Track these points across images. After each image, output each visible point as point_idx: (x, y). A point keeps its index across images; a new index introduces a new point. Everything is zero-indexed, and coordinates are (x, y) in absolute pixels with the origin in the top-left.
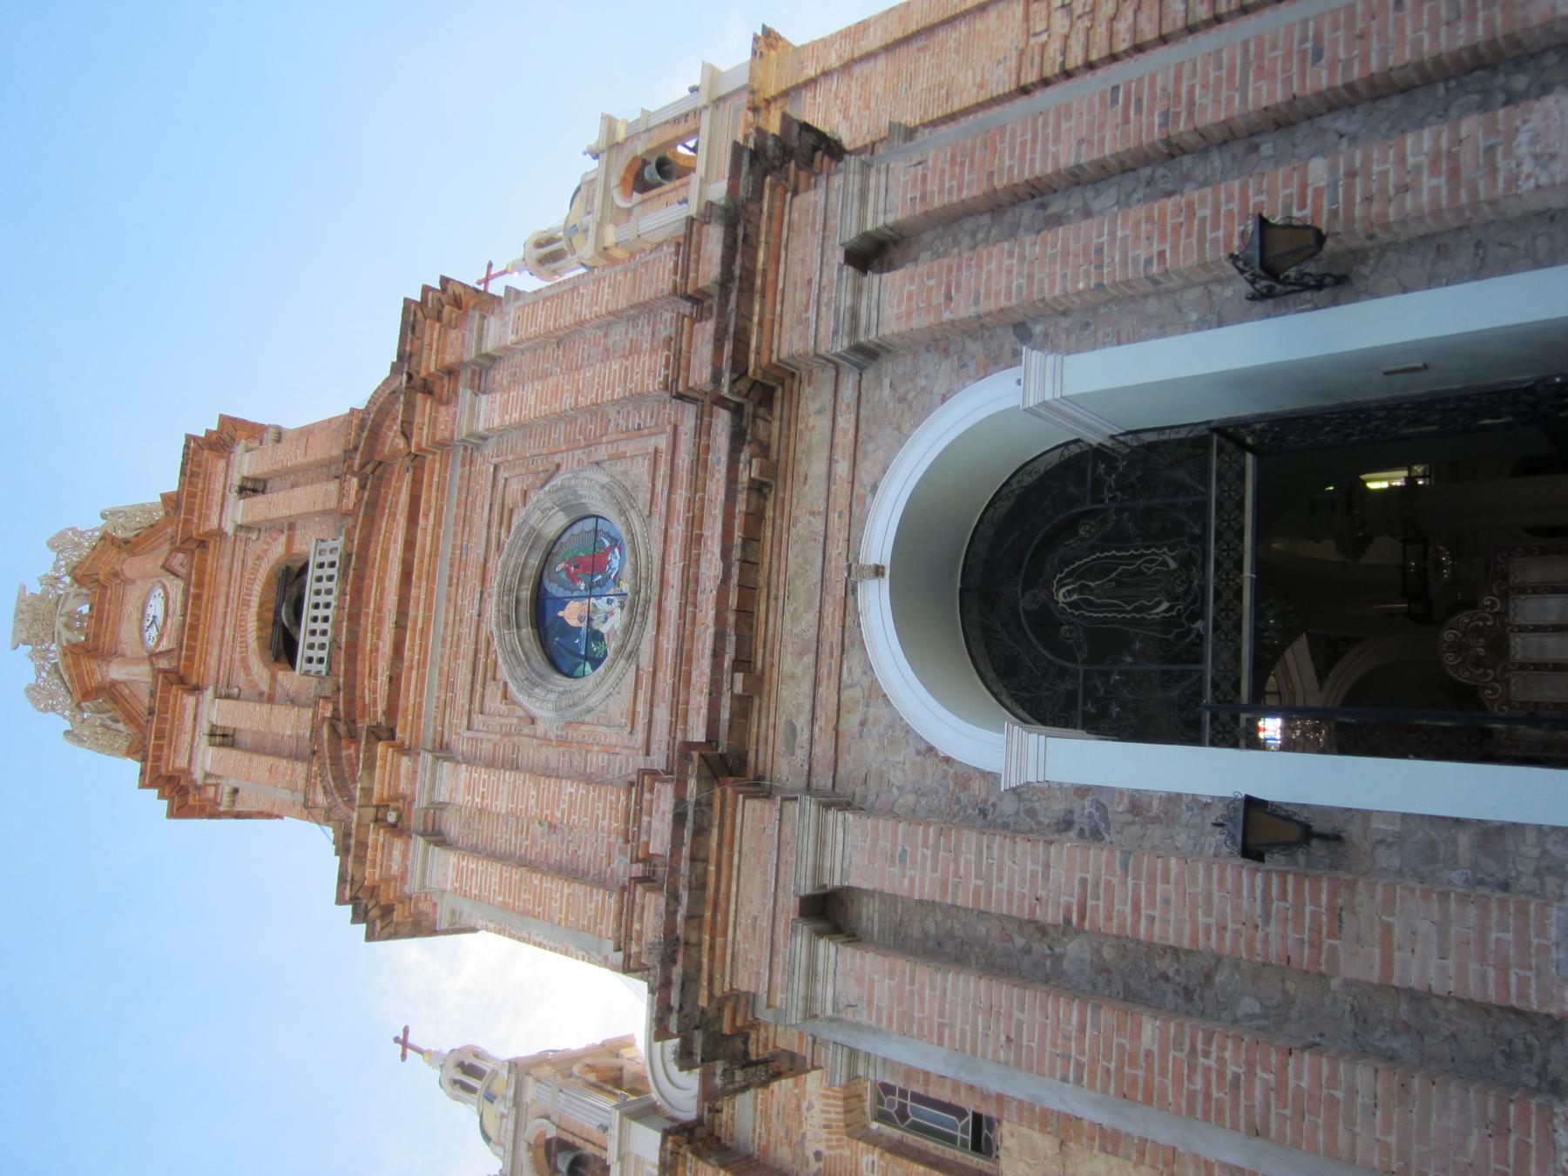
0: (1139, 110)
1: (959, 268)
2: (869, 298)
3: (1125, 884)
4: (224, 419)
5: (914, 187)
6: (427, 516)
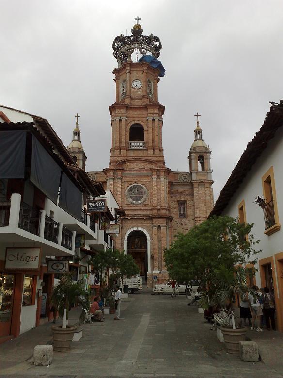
4: (165, 107)
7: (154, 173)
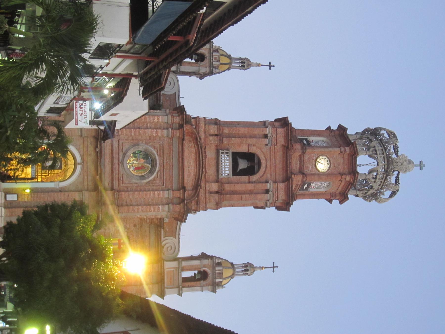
4: (289, 210)
7: (178, 194)
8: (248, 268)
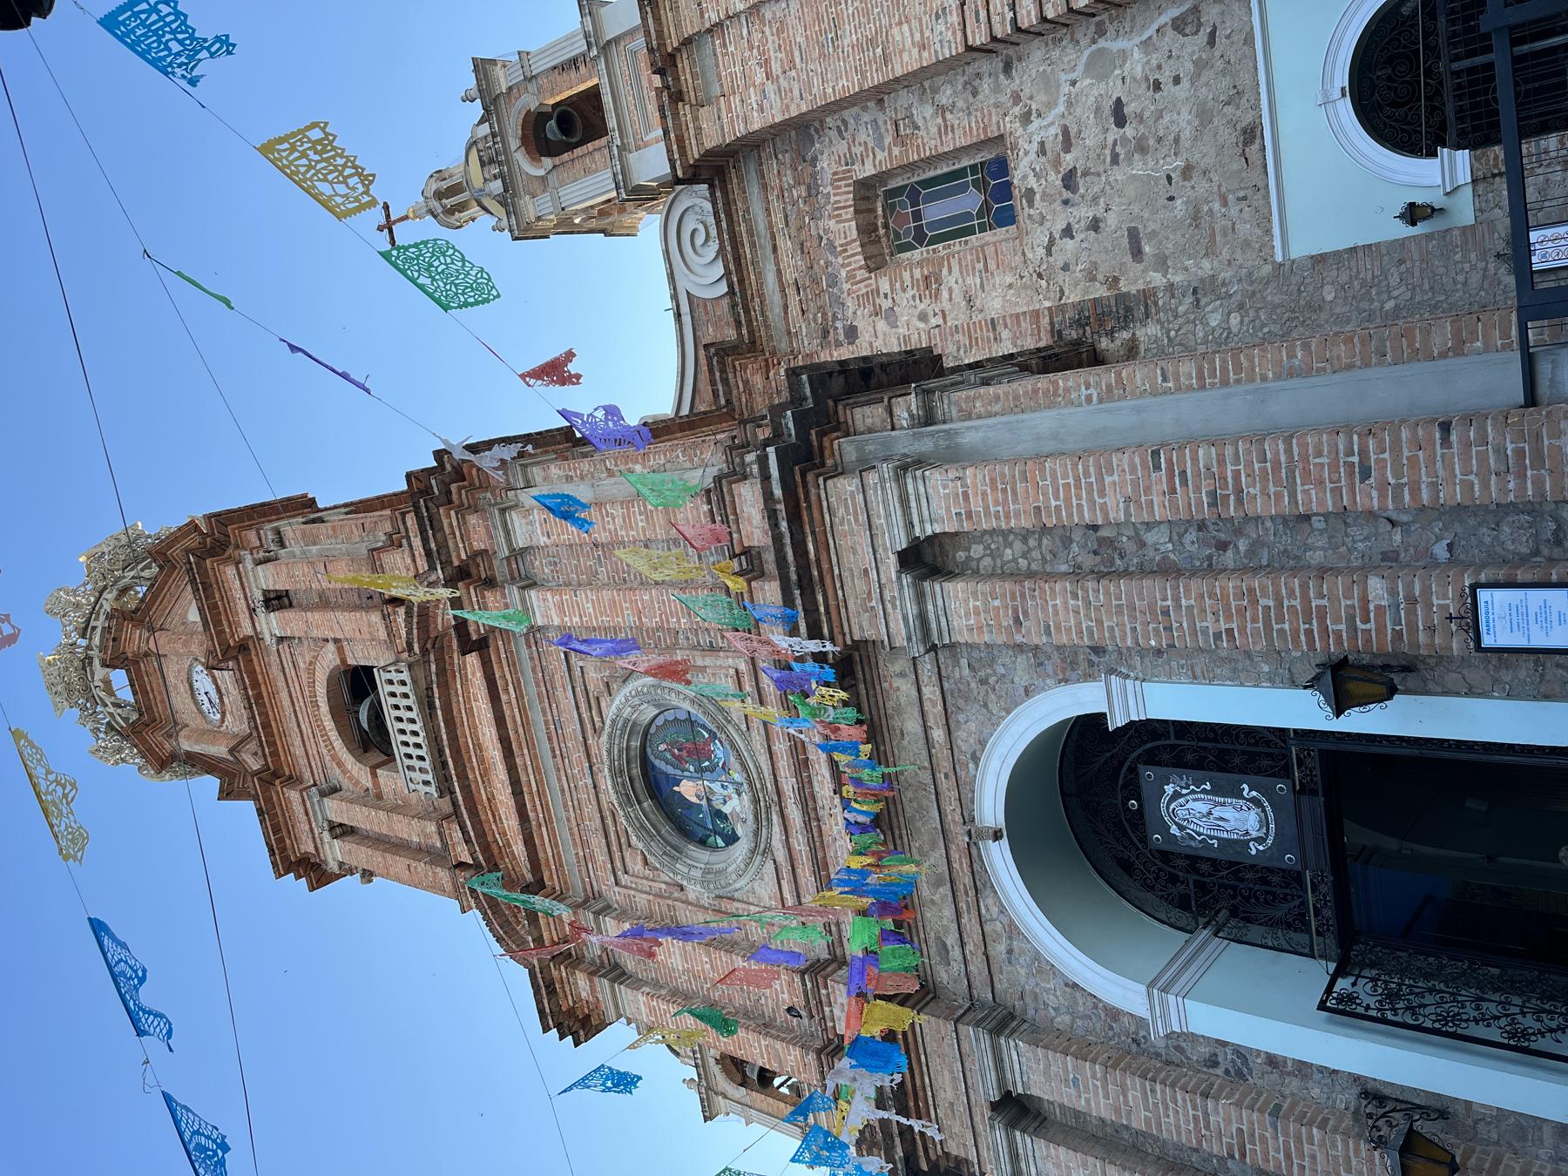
0: (1184, 482)
1: (1023, 596)
2: (935, 606)
3: (1277, 1138)
5: (957, 503)
6: (506, 690)
8: (435, 204)
